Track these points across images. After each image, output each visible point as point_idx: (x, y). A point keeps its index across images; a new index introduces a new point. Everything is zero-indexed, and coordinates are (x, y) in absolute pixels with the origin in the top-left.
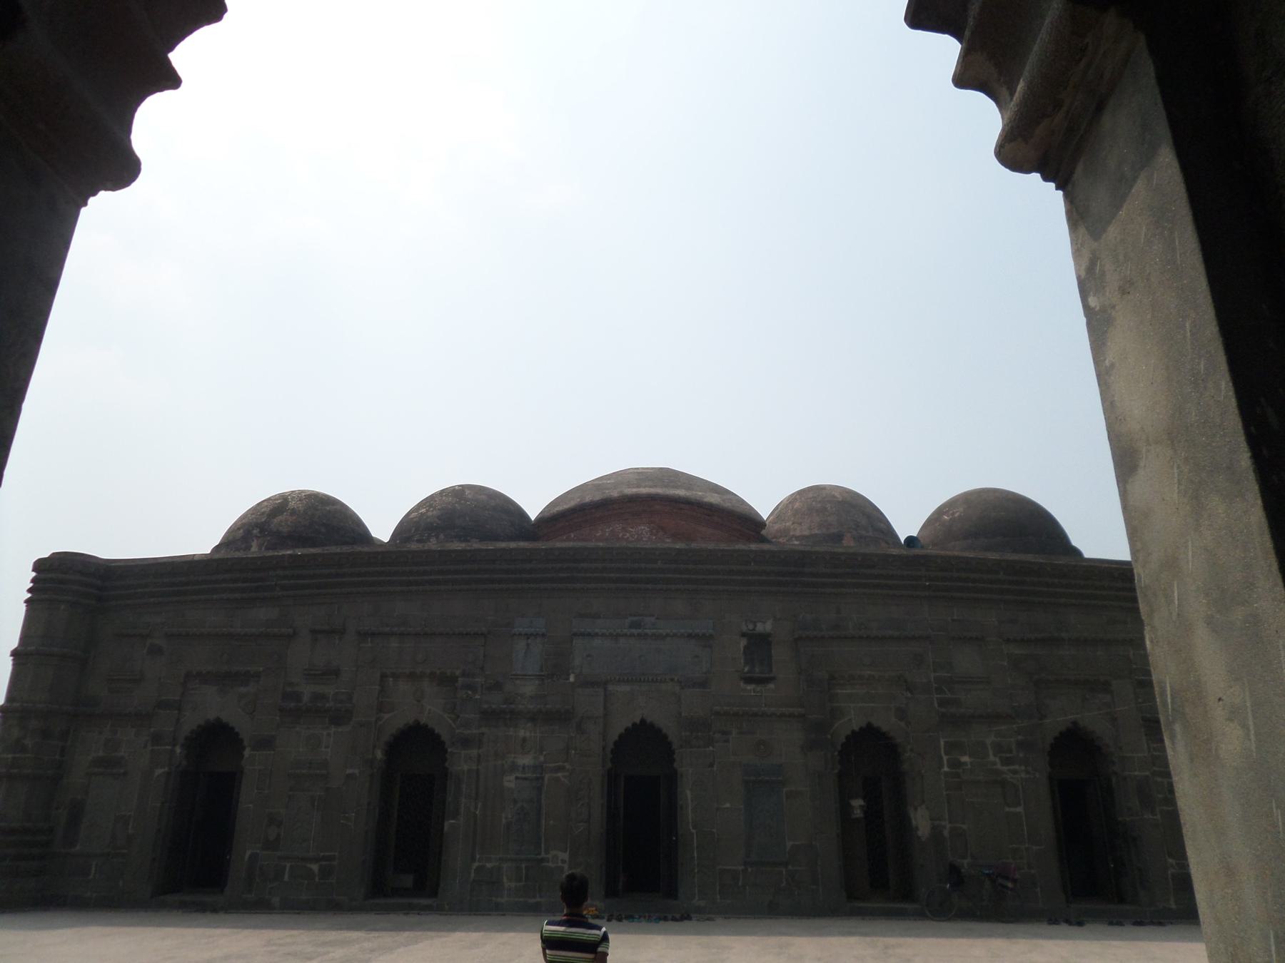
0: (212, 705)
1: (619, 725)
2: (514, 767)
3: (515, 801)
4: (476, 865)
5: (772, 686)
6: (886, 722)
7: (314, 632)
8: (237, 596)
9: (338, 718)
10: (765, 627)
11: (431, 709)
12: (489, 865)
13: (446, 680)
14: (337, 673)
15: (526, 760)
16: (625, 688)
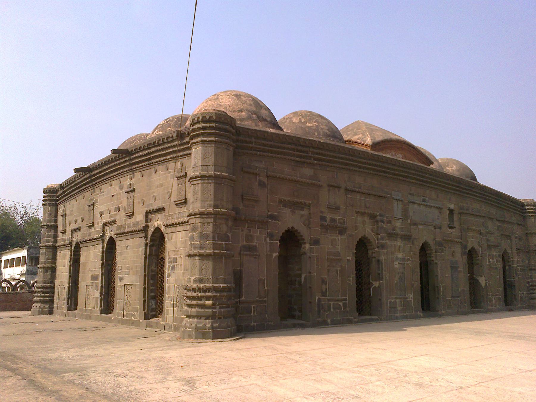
0: (291, 220)
1: (422, 242)
2: (397, 259)
3: (398, 273)
4: (389, 300)
5: (454, 230)
6: (476, 247)
7: (330, 186)
8: (299, 159)
9: (342, 231)
10: (452, 207)
11: (366, 229)
12: (393, 301)
13: (373, 217)
14: (338, 208)
15: (400, 256)
16: (421, 227)
